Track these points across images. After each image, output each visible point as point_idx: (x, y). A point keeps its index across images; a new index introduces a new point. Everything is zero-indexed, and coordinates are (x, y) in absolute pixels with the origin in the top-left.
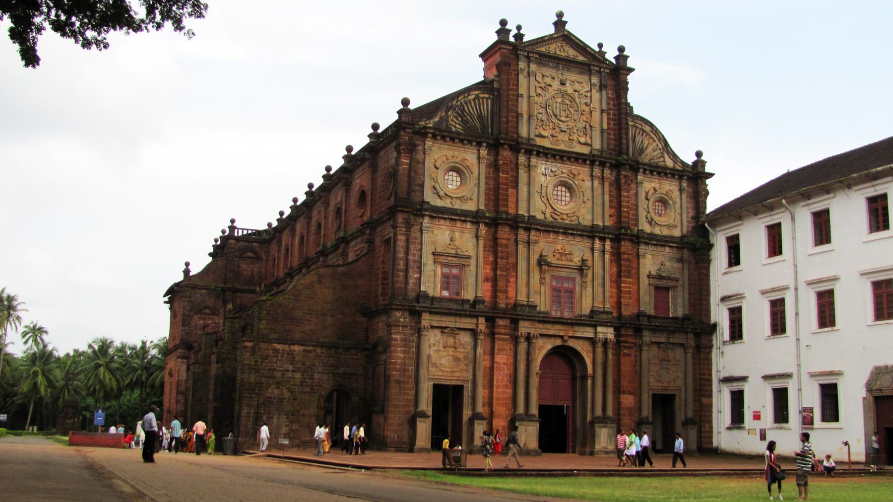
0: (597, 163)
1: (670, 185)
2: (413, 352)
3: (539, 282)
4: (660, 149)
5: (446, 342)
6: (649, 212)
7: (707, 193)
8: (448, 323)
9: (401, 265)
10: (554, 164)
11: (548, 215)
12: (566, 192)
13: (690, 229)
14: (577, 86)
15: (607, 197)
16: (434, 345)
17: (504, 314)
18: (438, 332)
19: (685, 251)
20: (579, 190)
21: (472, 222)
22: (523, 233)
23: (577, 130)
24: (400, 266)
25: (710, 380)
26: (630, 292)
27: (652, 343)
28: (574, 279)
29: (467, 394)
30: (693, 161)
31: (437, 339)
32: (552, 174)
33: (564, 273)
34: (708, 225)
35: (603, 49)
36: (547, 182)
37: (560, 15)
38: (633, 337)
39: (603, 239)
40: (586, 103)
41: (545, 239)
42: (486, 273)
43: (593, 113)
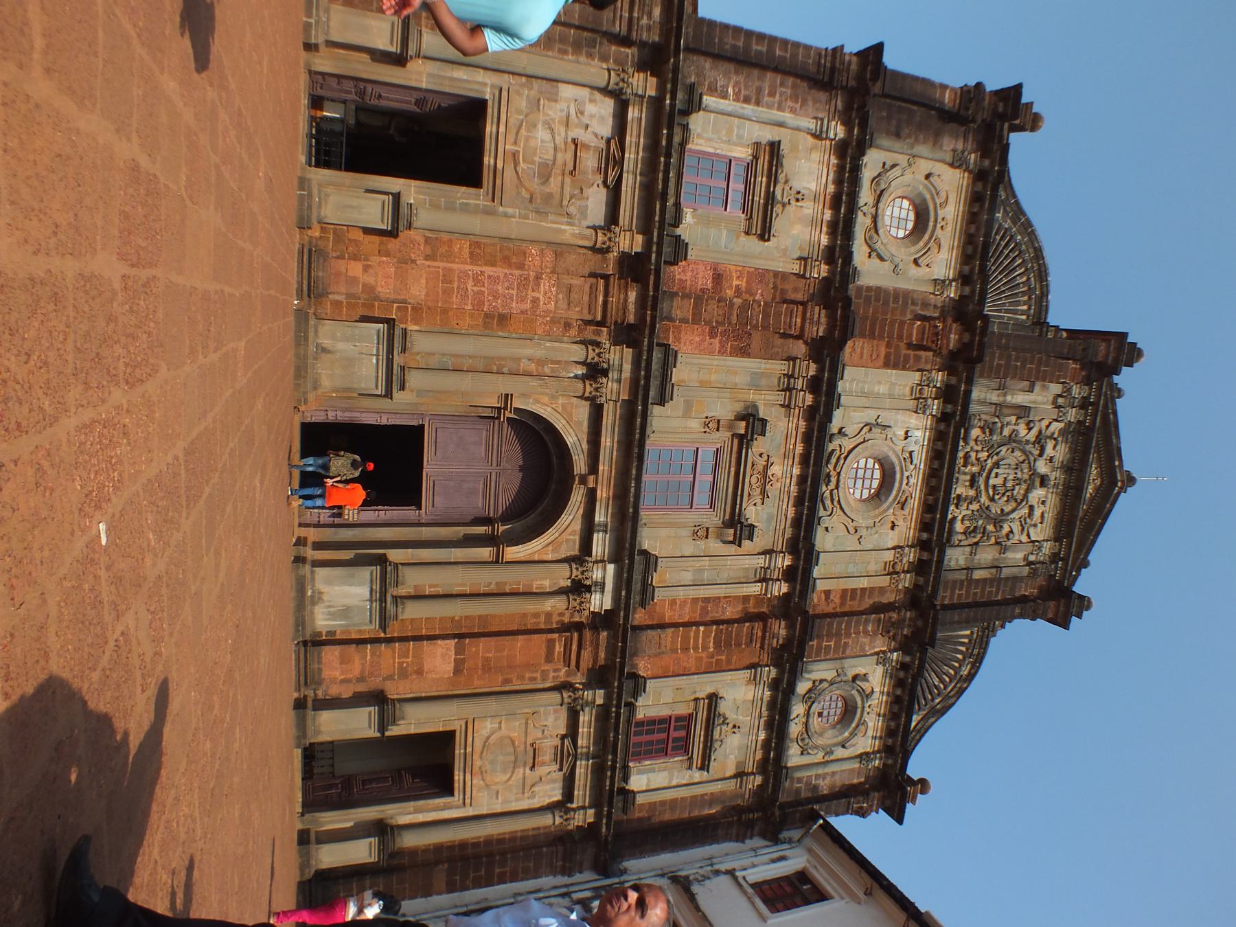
0: (925, 556)
1: (875, 730)
3: (710, 414)
5: (586, 147)
8: (633, 149)
14: (1037, 513)
15: (864, 583)
16: (582, 113)
17: (651, 303)
19: (759, 780)
20: (876, 516)
26: (687, 649)
29: (461, 193)
38: (590, 666)
39: (789, 575)
40: (1012, 532)
41: (794, 432)
42: (731, 277)
43: (998, 547)
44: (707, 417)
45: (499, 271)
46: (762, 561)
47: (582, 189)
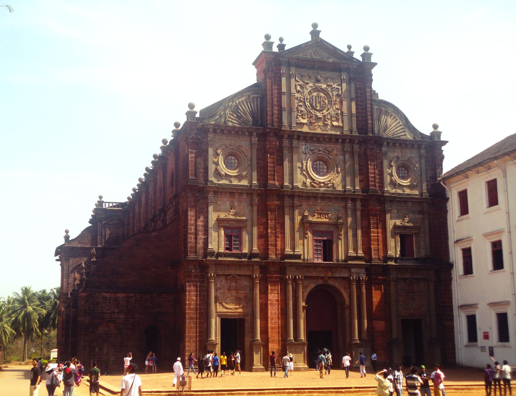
0: (348, 141)
2: (204, 294)
4: (401, 125)
5: (230, 285)
6: (393, 176)
7: (443, 157)
9: (192, 229)
10: (312, 144)
11: (308, 184)
12: (323, 165)
13: (429, 187)
15: (357, 167)
16: (220, 288)
17: (274, 263)
18: (223, 279)
19: (425, 204)
20: (333, 164)
21: (247, 194)
22: (288, 199)
23: (331, 116)
24: (192, 230)
25: (451, 307)
27: (398, 278)
28: (332, 232)
29: (247, 325)
30: (431, 132)
31: (223, 284)
32: (311, 152)
33: (323, 228)
34: (443, 183)
35: (352, 50)
36: (307, 158)
37: (315, 26)
39: (354, 200)
40: (337, 94)
44: (304, 237)
45: (269, 312)
46: (349, 212)
47: (241, 287)
